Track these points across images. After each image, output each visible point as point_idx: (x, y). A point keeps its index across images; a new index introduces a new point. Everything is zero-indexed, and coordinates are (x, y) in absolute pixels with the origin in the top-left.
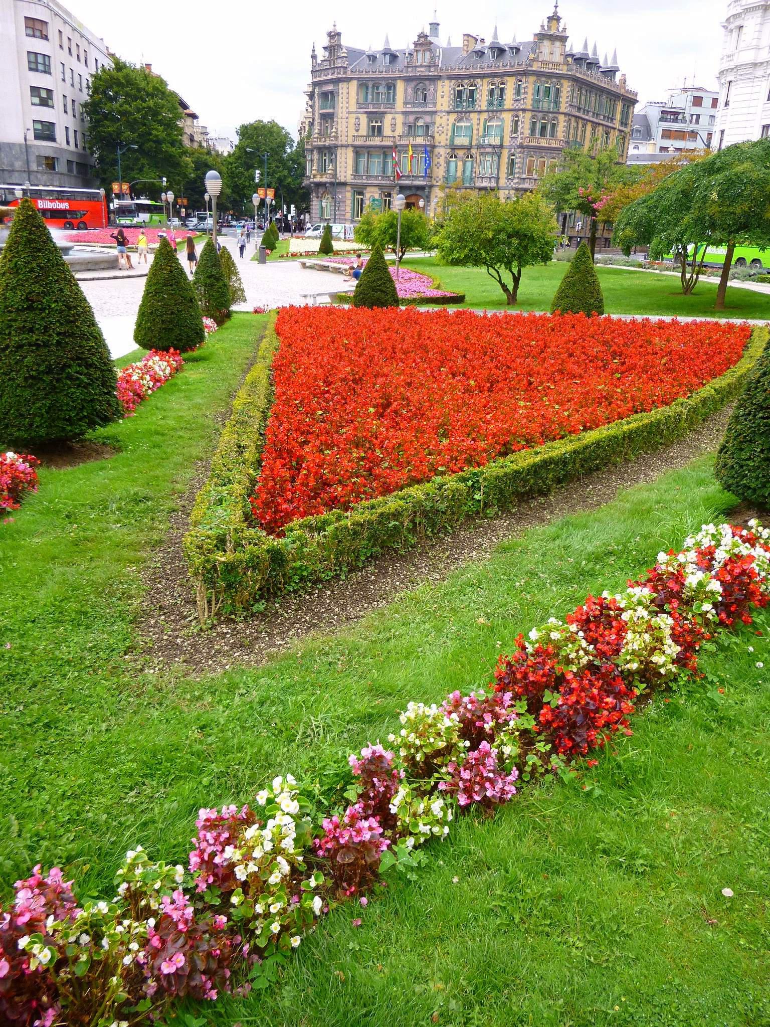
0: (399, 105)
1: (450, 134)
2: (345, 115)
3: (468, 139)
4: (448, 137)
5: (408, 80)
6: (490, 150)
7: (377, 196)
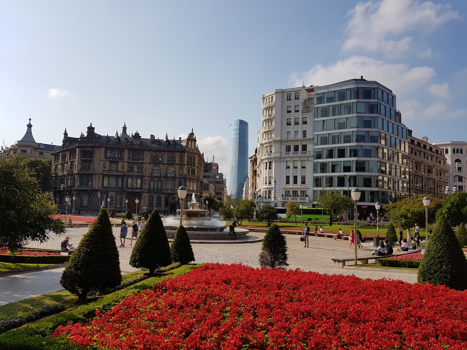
0: (126, 159)
1: (150, 171)
2: (98, 161)
3: (159, 174)
4: (150, 173)
5: (130, 150)
6: (171, 179)
7: (114, 196)
